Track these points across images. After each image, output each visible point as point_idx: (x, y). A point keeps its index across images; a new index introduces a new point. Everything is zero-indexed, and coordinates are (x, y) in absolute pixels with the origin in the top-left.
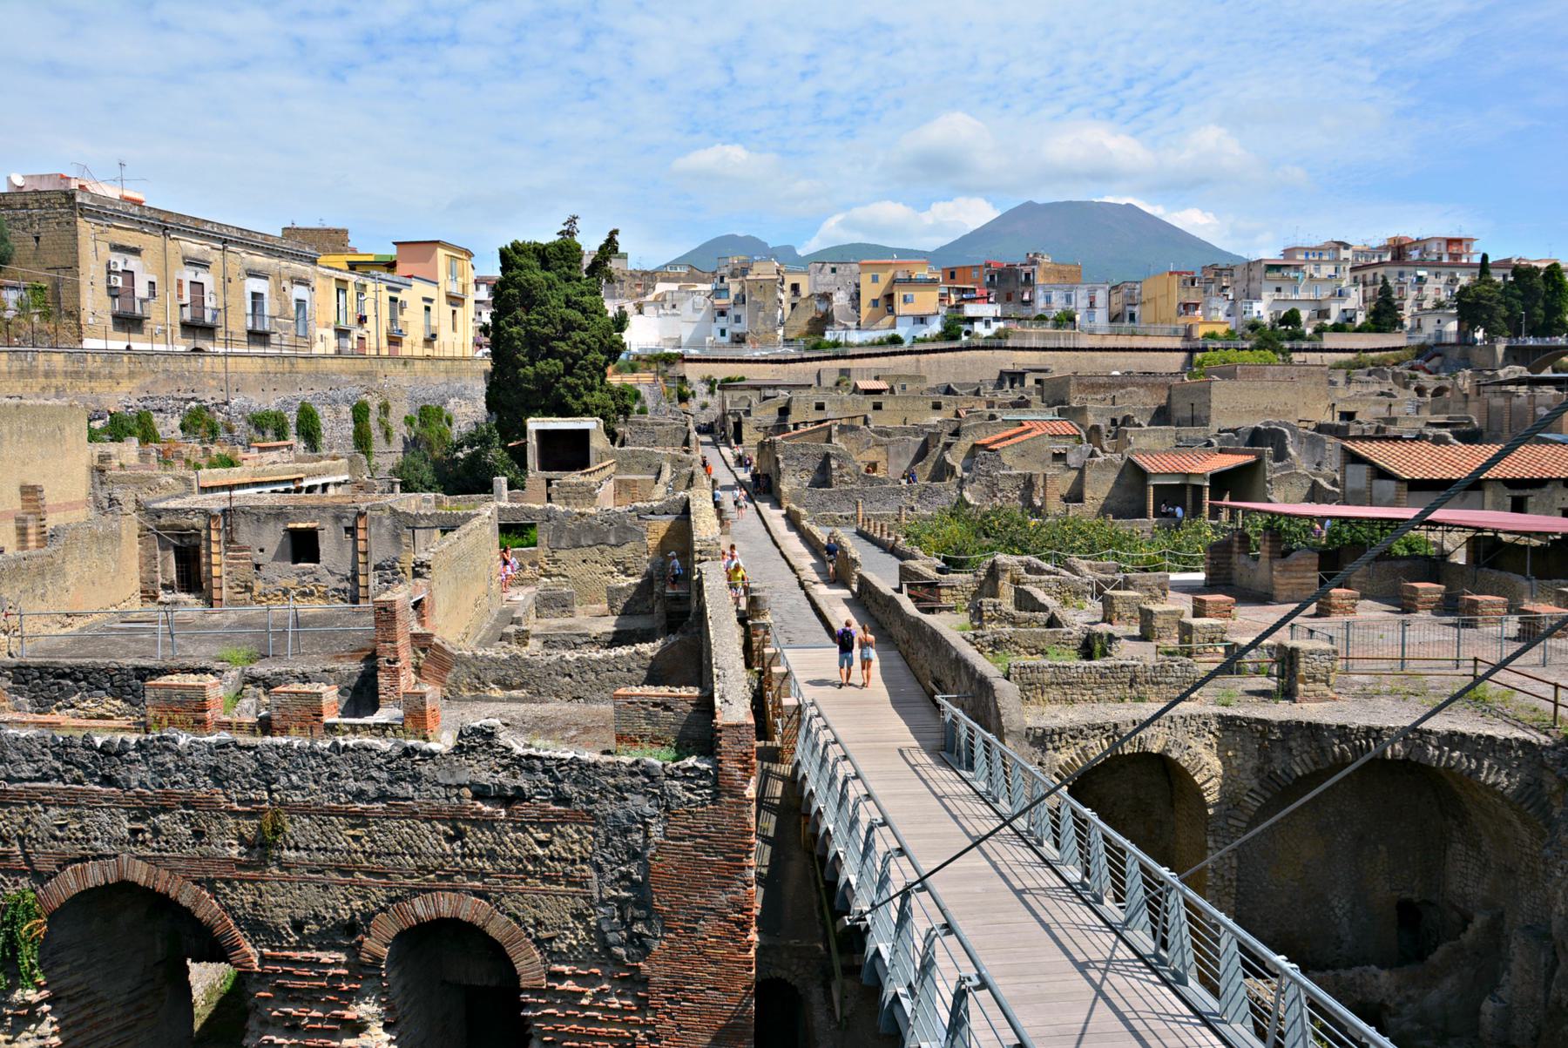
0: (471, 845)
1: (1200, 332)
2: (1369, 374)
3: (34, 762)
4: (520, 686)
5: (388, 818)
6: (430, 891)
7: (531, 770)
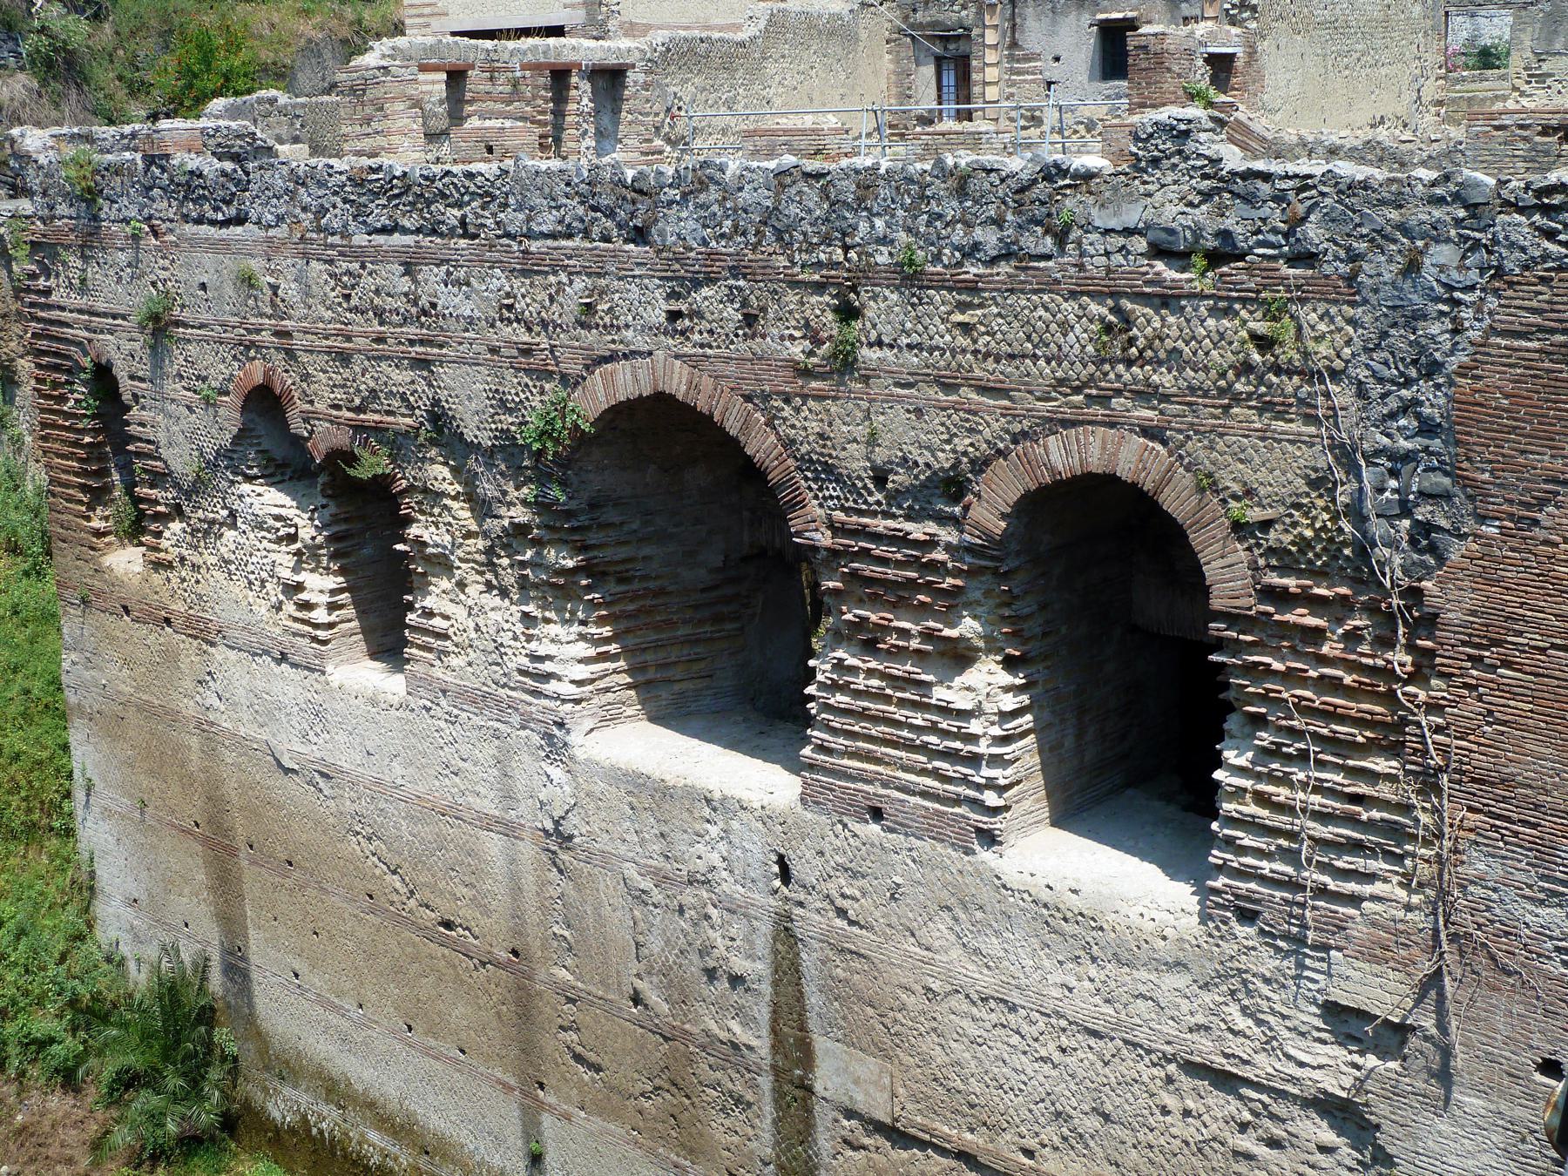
5: (1012, 291)
7: (1249, 199)
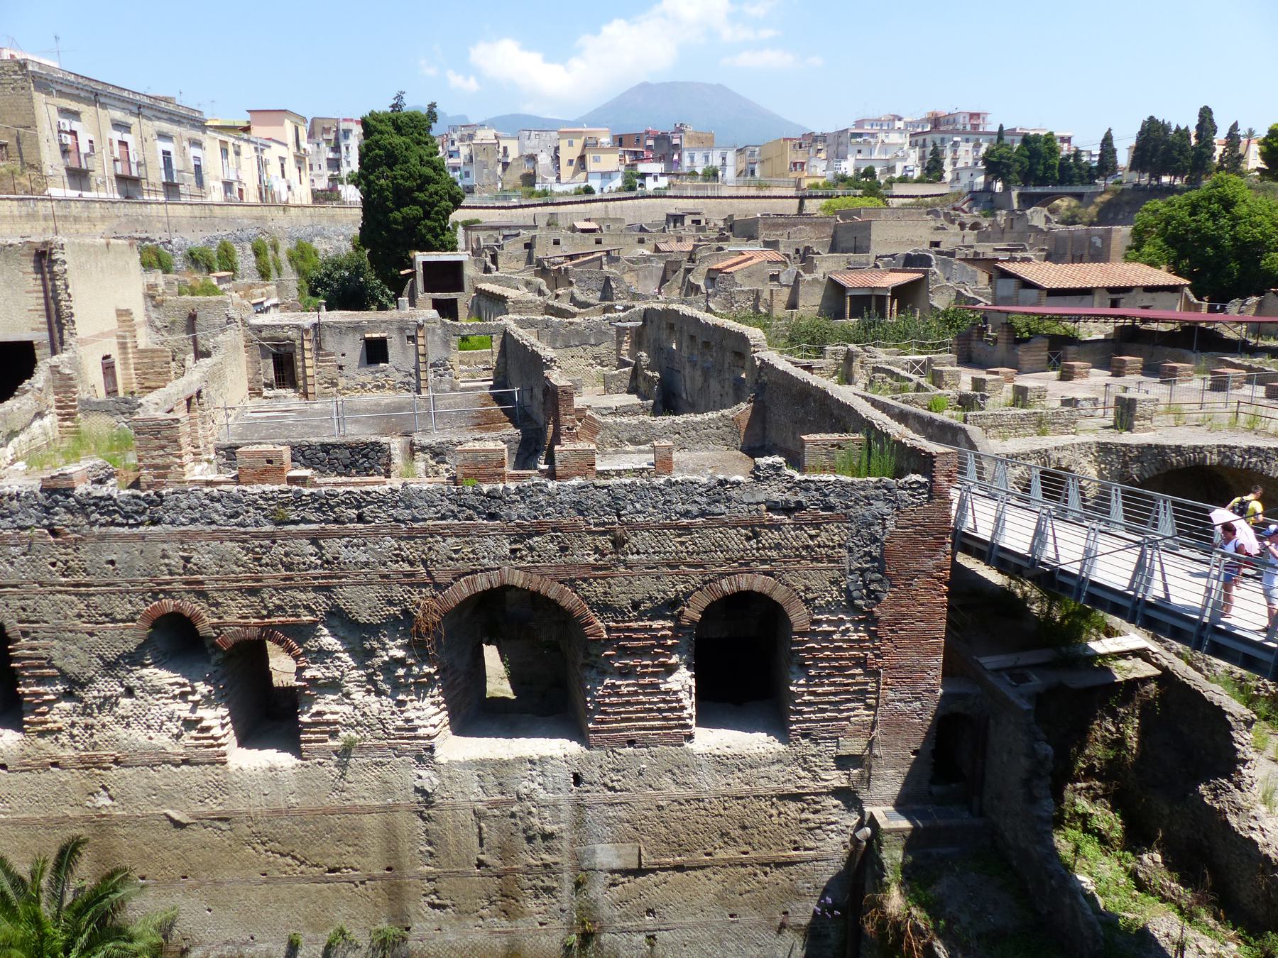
0: (764, 542)
1: (805, 184)
2: (928, 213)
3: (435, 507)
4: (645, 443)
6: (732, 574)
7: (807, 490)
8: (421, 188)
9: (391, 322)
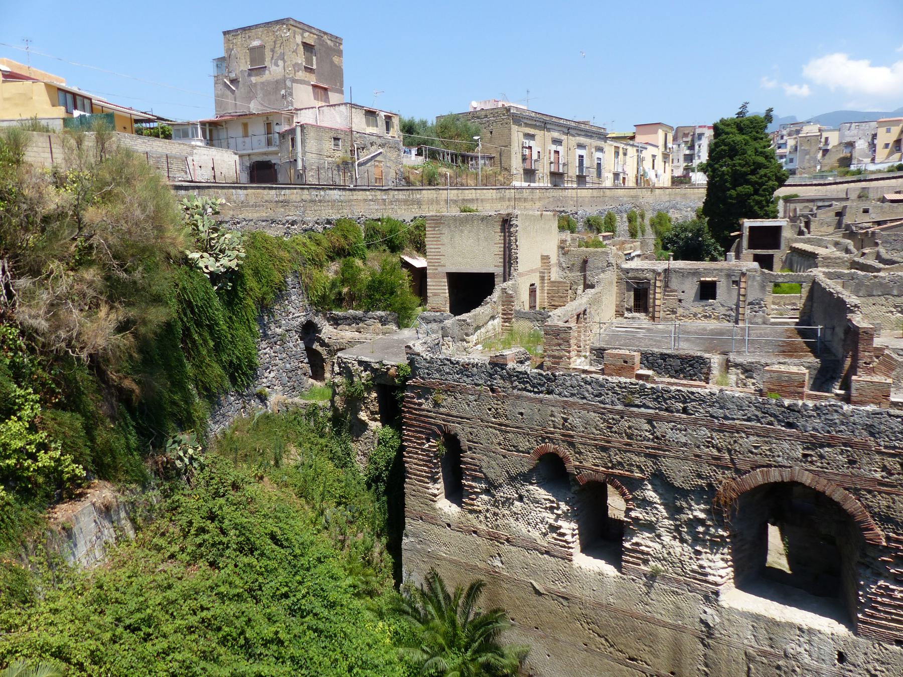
3: (743, 410)
8: (753, 172)
9: (721, 270)
